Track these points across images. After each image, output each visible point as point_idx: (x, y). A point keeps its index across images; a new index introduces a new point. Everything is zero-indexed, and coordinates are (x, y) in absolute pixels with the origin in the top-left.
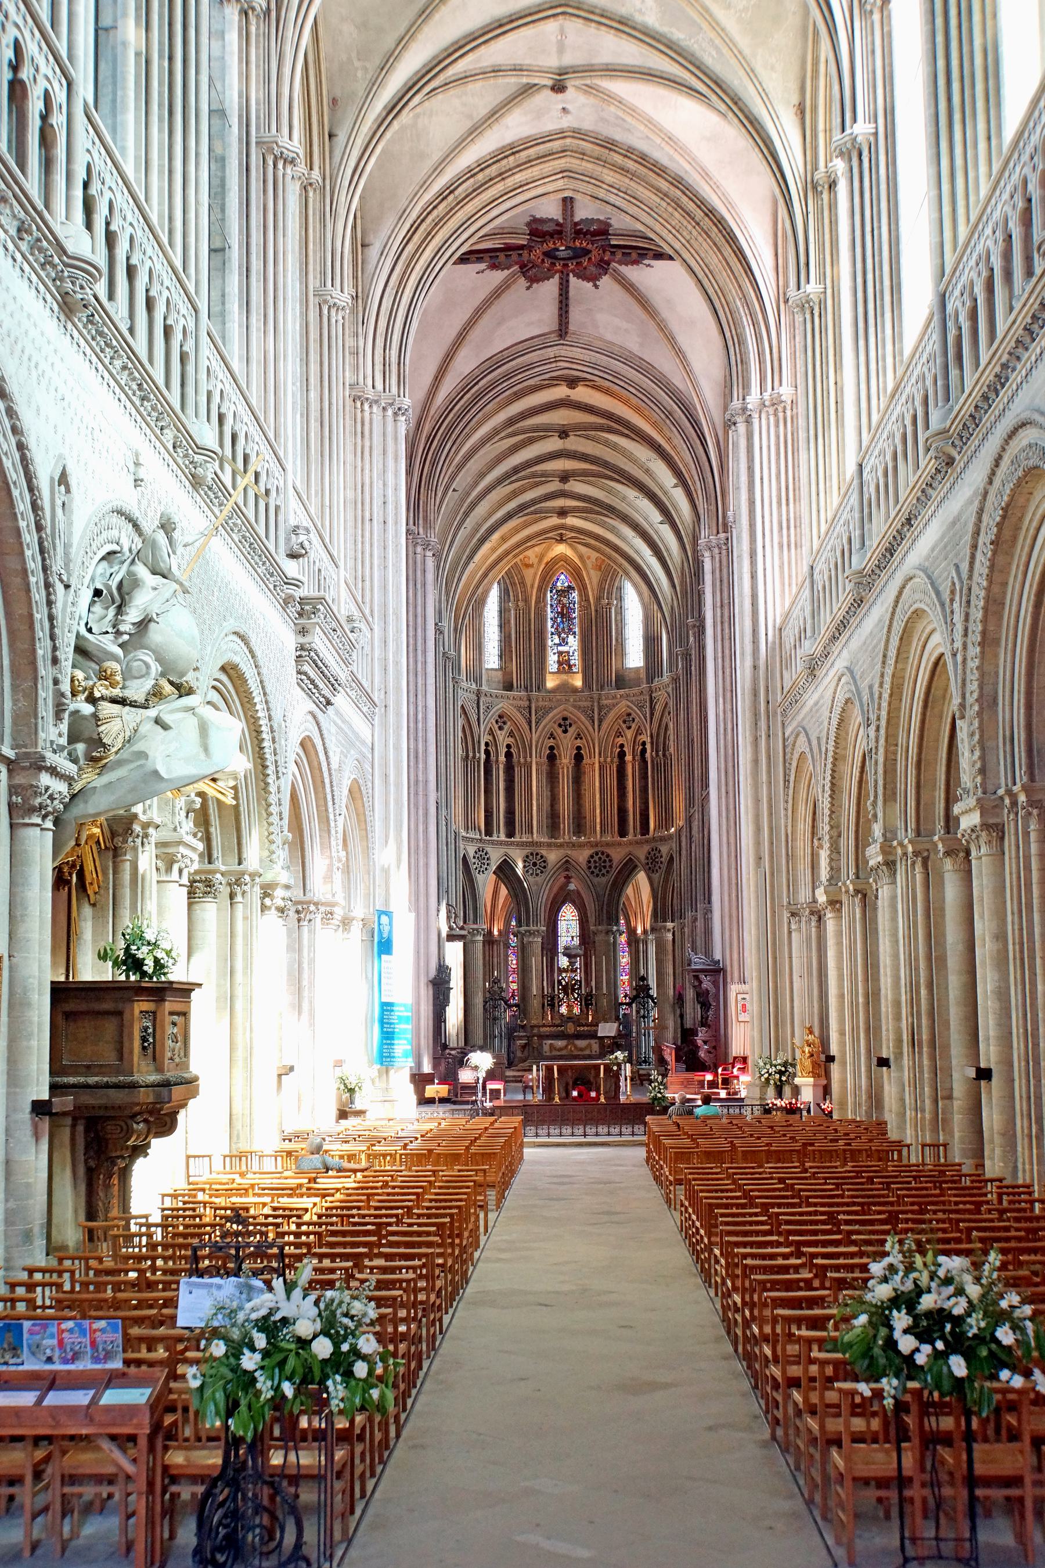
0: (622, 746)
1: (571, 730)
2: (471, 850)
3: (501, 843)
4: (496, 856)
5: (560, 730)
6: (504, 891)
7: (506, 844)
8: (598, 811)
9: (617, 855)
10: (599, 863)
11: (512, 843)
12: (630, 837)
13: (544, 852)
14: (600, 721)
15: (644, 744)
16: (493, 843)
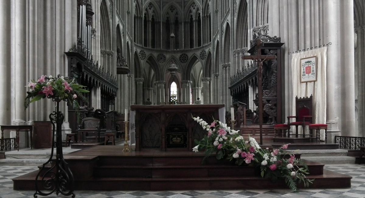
0: (192, 16)
1: (175, 11)
2: (139, 51)
3: (149, 50)
4: (147, 53)
5: (170, 11)
6: (153, 72)
7: (151, 50)
8: (183, 39)
9: (190, 55)
10: (183, 58)
11: (153, 50)
12: (195, 48)
13: (165, 55)
14: (184, 7)
15: (199, 14)
16: (147, 49)
